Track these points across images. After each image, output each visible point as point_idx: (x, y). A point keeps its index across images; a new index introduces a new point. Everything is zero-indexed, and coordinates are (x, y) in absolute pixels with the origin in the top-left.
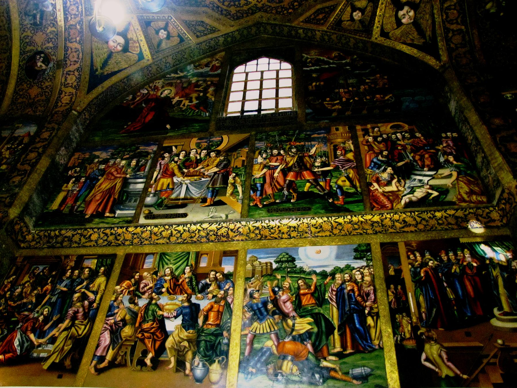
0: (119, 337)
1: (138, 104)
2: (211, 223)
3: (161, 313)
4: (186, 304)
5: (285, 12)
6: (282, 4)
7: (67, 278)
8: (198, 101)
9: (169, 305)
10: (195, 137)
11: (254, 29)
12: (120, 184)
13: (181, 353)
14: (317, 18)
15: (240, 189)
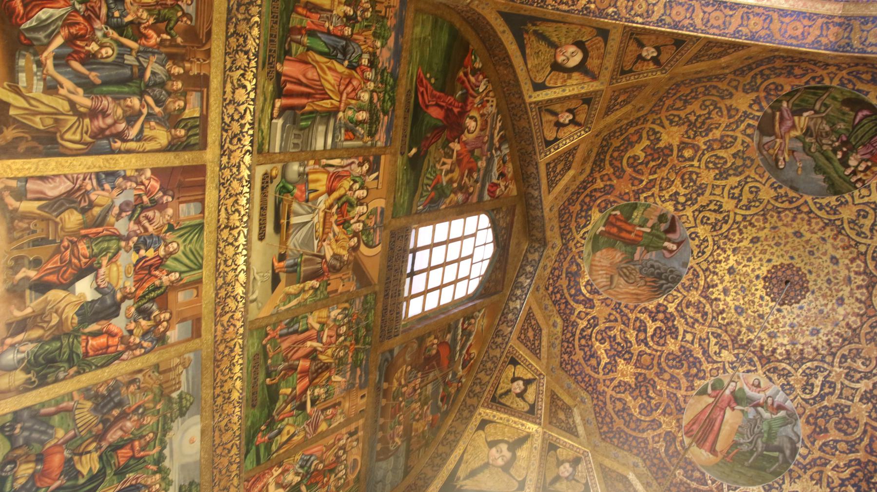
0: (63, 208)
1: (463, 82)
2: (246, 285)
3: (105, 261)
4: (119, 296)
5: (551, 281)
6: (564, 275)
7: (168, 71)
8: (444, 184)
9: (118, 270)
10: (387, 203)
11: (539, 235)
12: (329, 106)
13: (38, 320)
14: (530, 329)
15: (294, 302)
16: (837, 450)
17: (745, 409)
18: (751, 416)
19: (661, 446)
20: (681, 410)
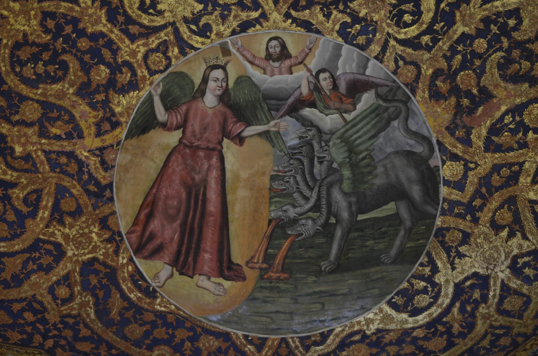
16: (527, 129)
17: (271, 127)
18: (292, 141)
19: (84, 305)
20: (102, 193)
